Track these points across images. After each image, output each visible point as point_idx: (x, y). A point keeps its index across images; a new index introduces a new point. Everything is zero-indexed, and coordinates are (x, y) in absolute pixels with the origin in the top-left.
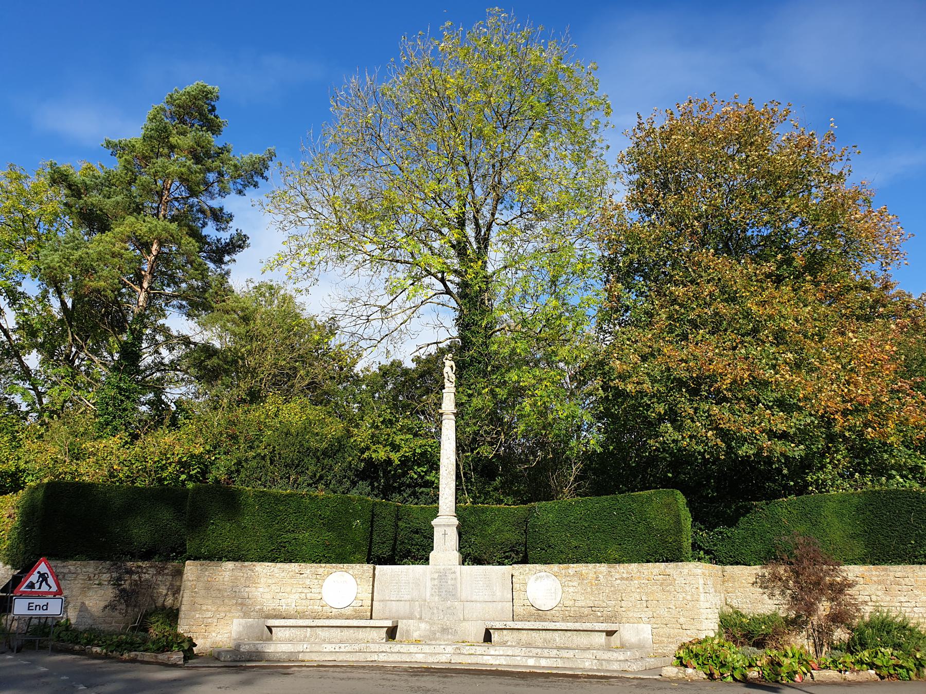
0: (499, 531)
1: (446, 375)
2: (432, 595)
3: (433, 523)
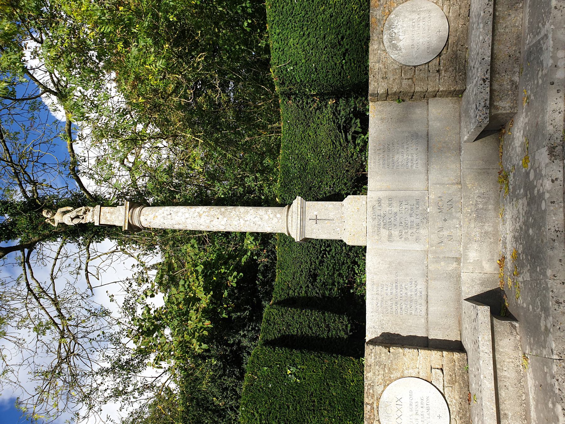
0: (315, 148)
1: (76, 222)
2: (417, 240)
3: (297, 239)
